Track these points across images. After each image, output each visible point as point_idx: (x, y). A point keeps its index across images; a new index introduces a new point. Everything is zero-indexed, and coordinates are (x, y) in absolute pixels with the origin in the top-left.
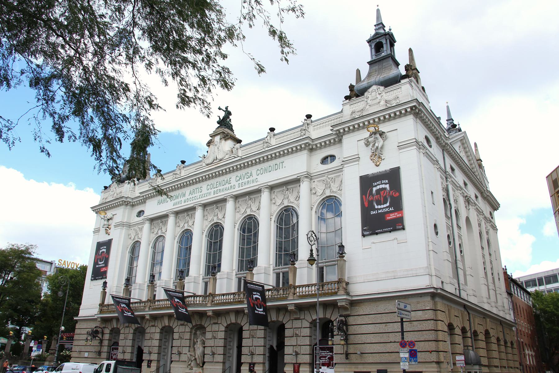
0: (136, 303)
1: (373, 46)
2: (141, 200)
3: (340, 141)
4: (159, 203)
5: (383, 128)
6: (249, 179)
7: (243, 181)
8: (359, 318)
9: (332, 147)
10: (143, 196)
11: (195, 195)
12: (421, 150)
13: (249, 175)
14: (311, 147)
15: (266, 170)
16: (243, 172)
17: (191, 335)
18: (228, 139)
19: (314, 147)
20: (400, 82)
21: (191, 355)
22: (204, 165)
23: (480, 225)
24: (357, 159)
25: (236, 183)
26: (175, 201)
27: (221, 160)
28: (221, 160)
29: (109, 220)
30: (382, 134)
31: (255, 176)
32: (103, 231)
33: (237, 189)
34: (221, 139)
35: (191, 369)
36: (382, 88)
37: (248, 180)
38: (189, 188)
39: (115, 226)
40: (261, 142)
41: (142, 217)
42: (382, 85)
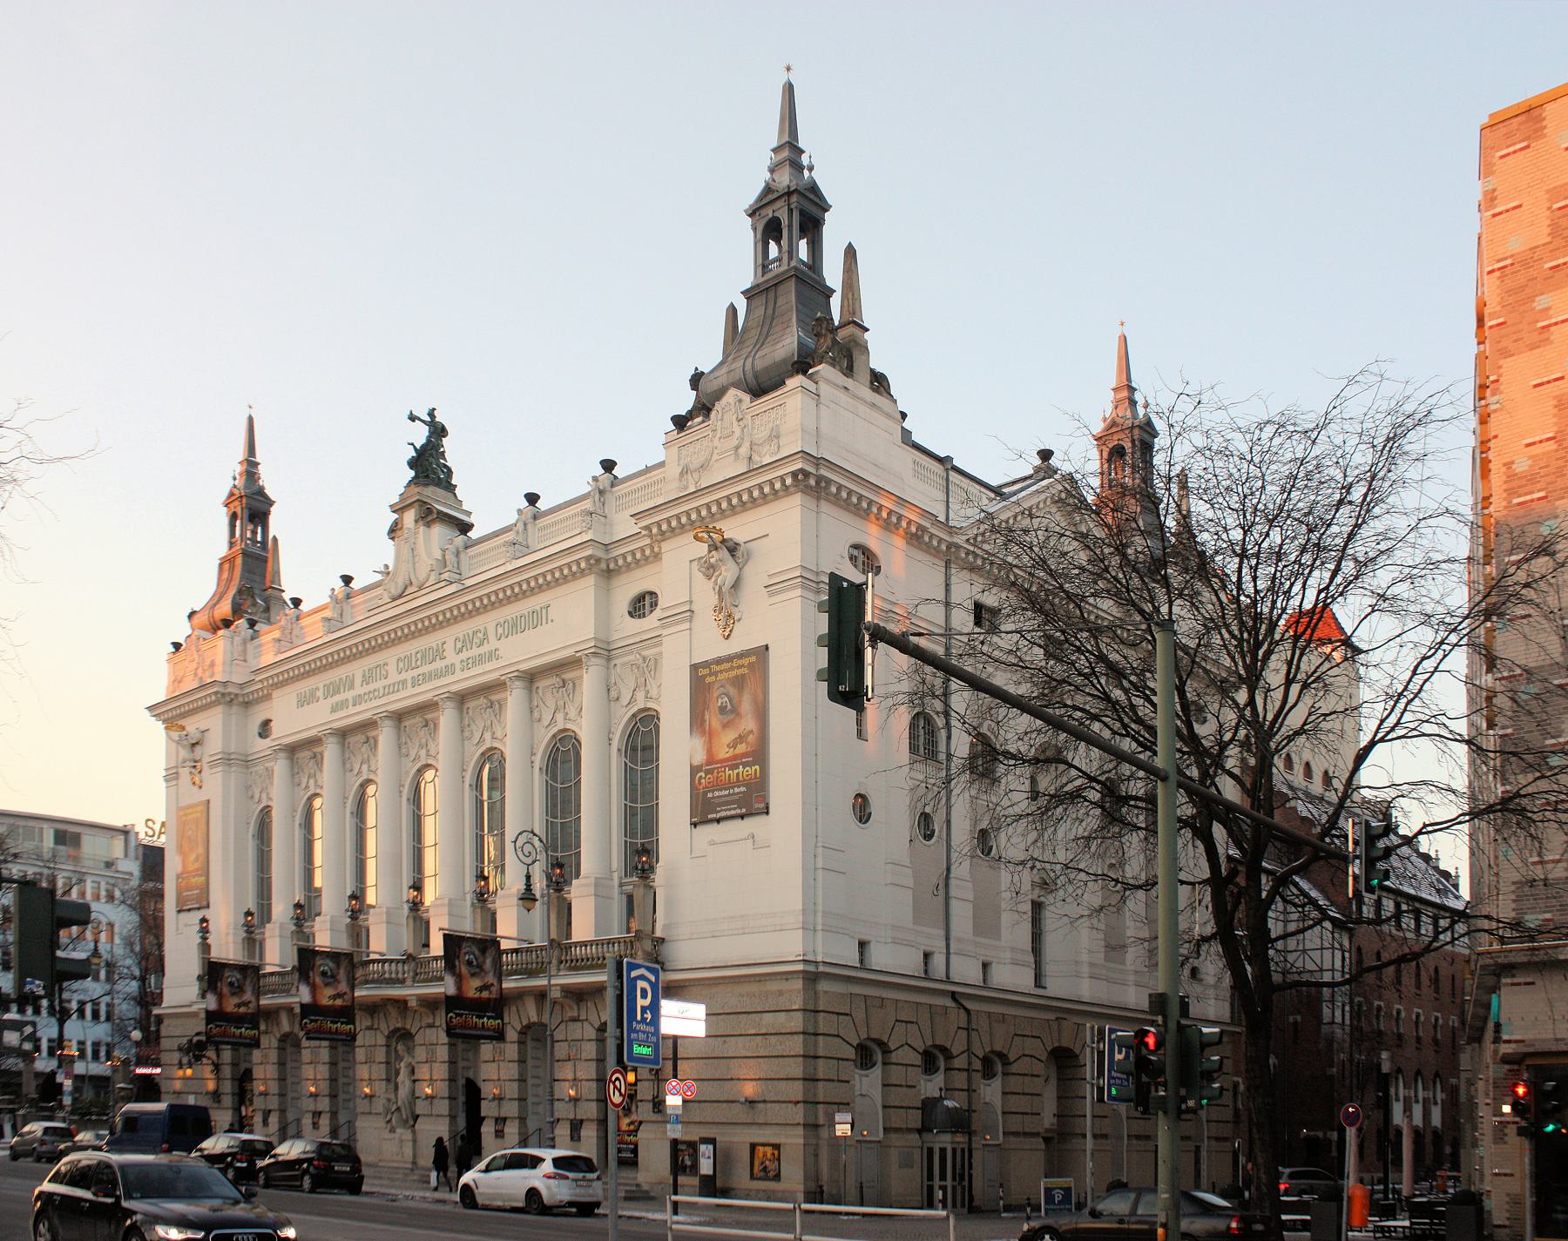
0: (272, 974)
3: (657, 557)
5: (734, 529)
6: (482, 650)
13: (480, 635)
14: (605, 566)
17: (388, 1053)
18: (433, 521)
25: (455, 661)
26: (337, 698)
29: (193, 745)
30: (733, 548)
32: (185, 772)
33: (459, 675)
35: (392, 1130)
39: (213, 765)
41: (267, 742)
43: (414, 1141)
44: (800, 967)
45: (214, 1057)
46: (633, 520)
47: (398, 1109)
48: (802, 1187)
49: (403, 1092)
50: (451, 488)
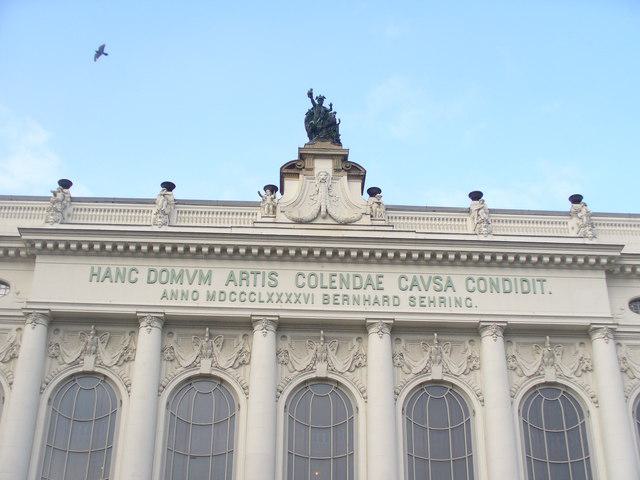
13: (444, 283)
15: (495, 286)
16: (426, 273)
33: (405, 307)
37: (442, 294)
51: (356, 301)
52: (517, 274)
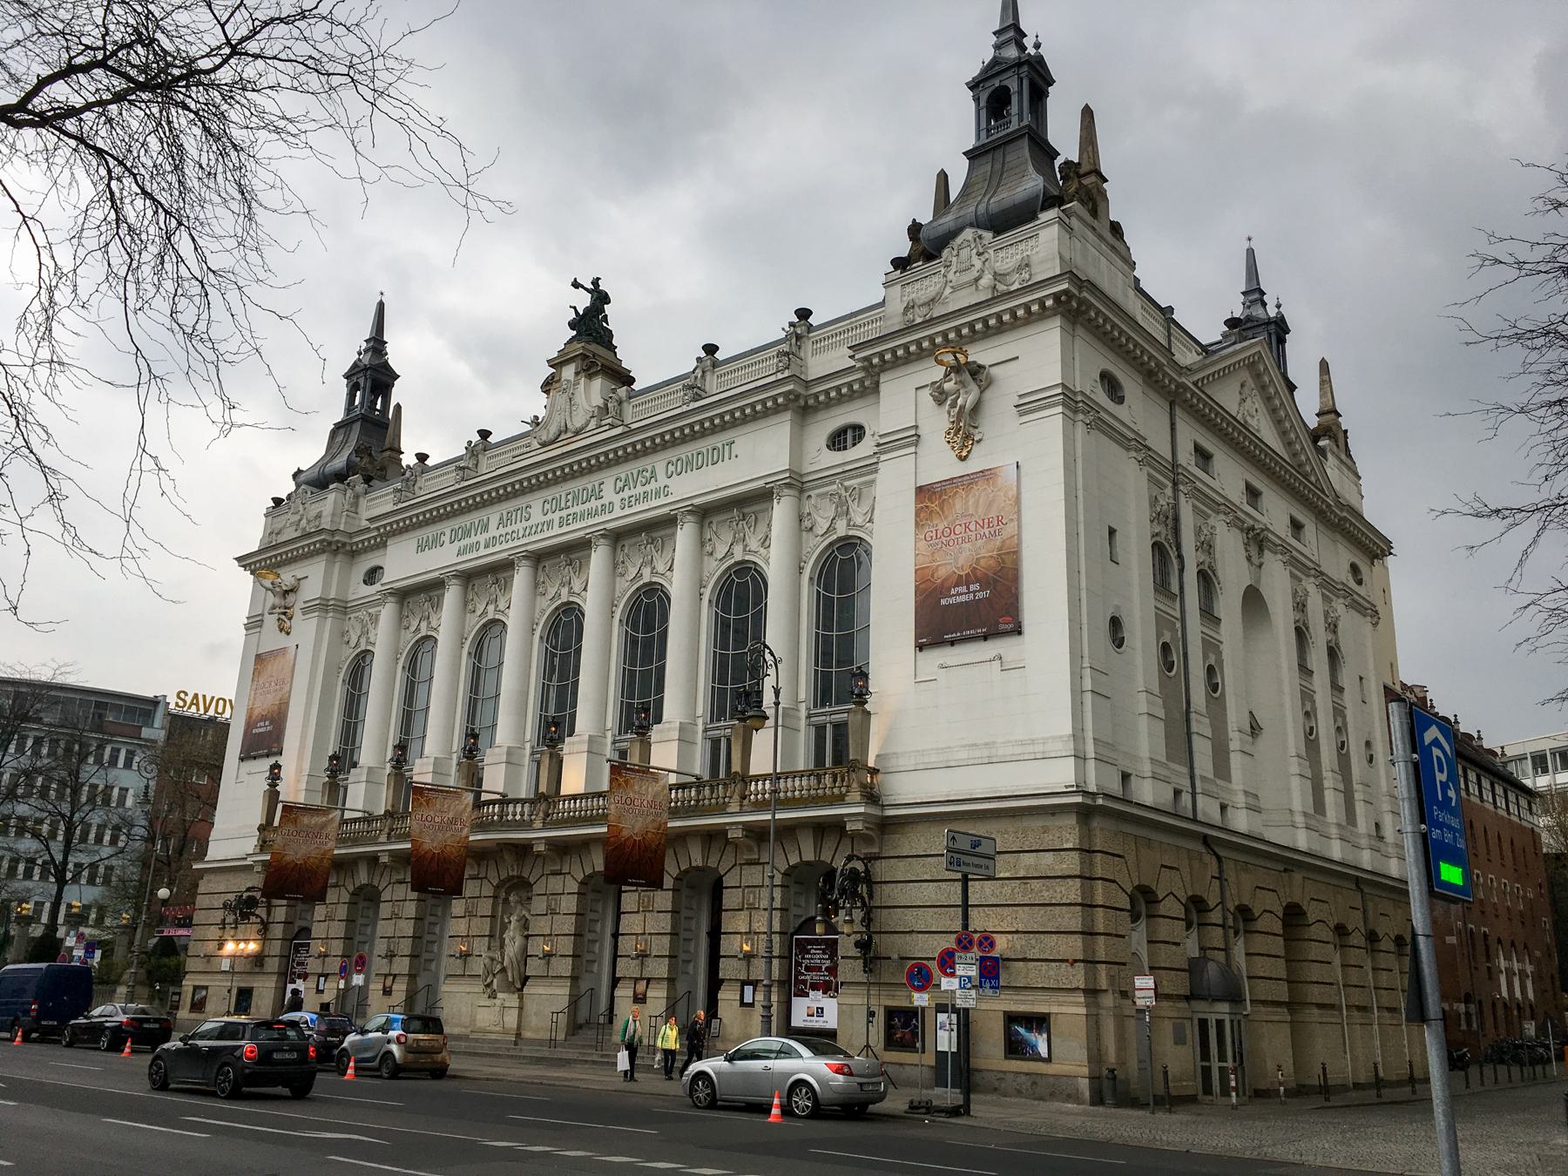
0: (355, 820)
1: (983, 103)
2: (375, 538)
3: (876, 389)
4: (421, 548)
5: (980, 354)
6: (647, 488)
7: (633, 492)
8: (901, 864)
9: (858, 404)
10: (378, 529)
11: (514, 527)
12: (1081, 417)
13: (648, 475)
14: (802, 404)
15: (689, 465)
16: (632, 468)
18: (596, 374)
19: (811, 402)
20: (1034, 217)
21: (492, 959)
22: (535, 445)
23: (1301, 607)
24: (913, 438)
25: (616, 499)
26: (463, 542)
27: (577, 433)
28: (577, 433)
29: (286, 592)
30: (976, 371)
31: (662, 480)
32: (271, 621)
33: (617, 513)
34: (577, 374)
35: (493, 996)
36: (988, 235)
38: (496, 508)
39: (305, 611)
40: (679, 385)
41: (377, 587)
42: (987, 229)
43: (521, 1008)
44: (1079, 799)
45: (264, 916)
46: (851, 353)
47: (504, 970)
48: (1085, 1071)
49: (512, 949)
50: (612, 348)
51: (582, 518)
52: (704, 445)
